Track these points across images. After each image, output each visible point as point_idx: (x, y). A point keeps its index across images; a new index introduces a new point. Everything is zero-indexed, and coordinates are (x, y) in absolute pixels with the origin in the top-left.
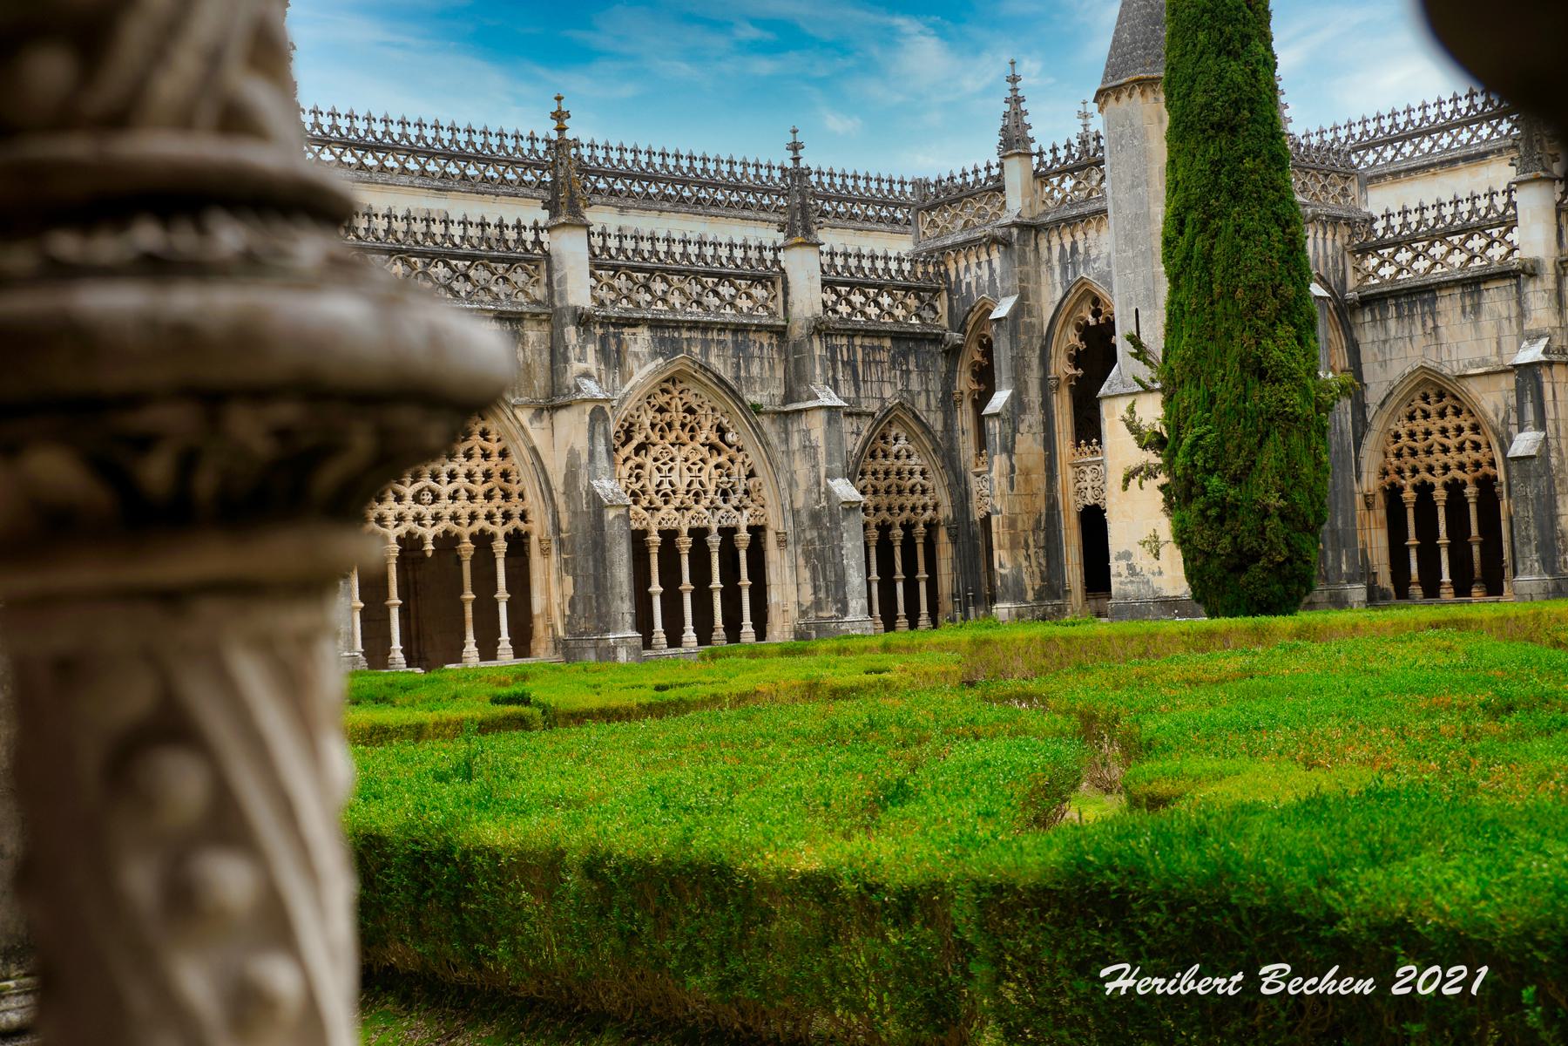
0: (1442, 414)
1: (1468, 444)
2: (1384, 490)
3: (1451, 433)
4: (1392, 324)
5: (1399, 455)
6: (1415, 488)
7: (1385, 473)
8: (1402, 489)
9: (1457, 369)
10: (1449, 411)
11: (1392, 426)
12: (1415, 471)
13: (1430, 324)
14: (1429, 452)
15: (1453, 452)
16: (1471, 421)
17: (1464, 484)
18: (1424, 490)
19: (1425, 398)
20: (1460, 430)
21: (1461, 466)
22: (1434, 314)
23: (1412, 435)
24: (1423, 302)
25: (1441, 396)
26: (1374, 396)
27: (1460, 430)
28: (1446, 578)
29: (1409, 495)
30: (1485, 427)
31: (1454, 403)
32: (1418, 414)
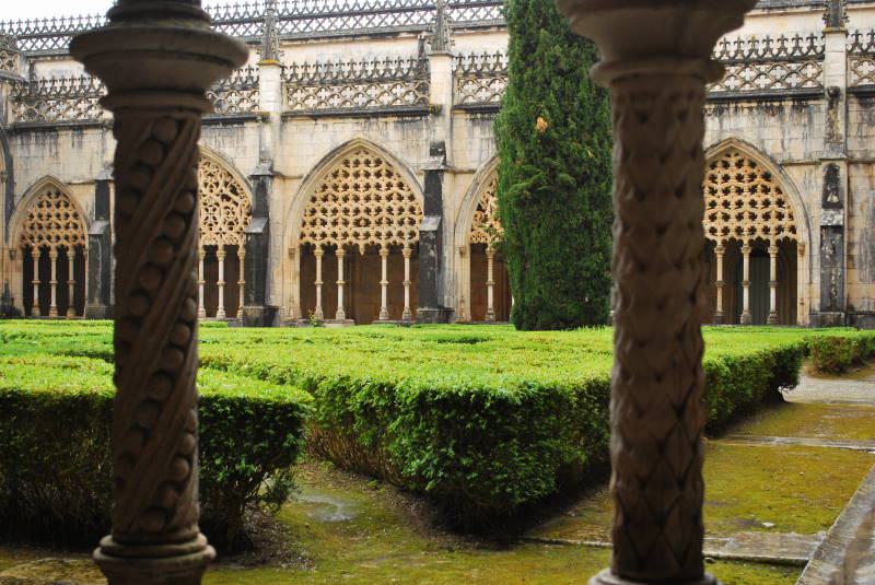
0: (58, 206)
1: (71, 225)
2: (22, 249)
3: (62, 217)
4: (32, 147)
5: (32, 228)
6: (40, 248)
7: (23, 238)
8: (32, 249)
9: (67, 180)
10: (62, 204)
11: (29, 210)
12: (40, 238)
13: (54, 150)
14: (49, 227)
15: (62, 229)
16: (73, 211)
17: (67, 249)
18: (45, 250)
19: (49, 195)
20: (67, 216)
21: (67, 238)
22: (56, 144)
23: (40, 216)
24: (52, 137)
25: (58, 194)
26: (19, 190)
27: (67, 216)
28: (53, 304)
29: (36, 253)
30: (81, 216)
31: (64, 199)
32: (45, 204)
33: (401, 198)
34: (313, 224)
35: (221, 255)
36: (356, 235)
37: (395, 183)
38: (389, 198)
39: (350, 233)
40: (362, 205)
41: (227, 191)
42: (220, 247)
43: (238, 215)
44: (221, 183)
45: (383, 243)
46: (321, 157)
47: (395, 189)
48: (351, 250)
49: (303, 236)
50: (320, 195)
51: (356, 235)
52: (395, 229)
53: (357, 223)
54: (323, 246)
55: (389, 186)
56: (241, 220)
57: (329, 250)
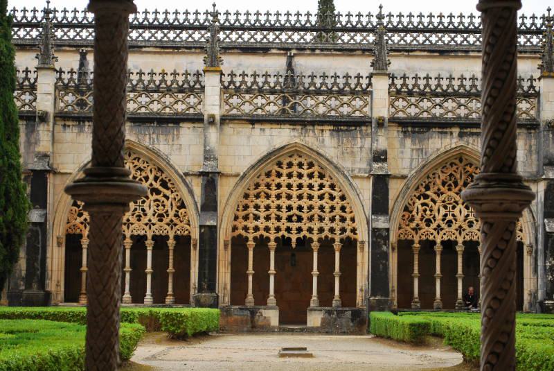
33: (332, 198)
34: (246, 218)
35: (149, 243)
36: (289, 230)
38: (321, 197)
39: (283, 227)
40: (295, 203)
41: (157, 185)
42: (149, 237)
43: (168, 206)
44: (151, 177)
45: (315, 237)
46: (259, 158)
47: (327, 189)
48: (284, 243)
49: (235, 229)
50: (253, 192)
51: (289, 230)
52: (327, 225)
53: (289, 219)
54: (255, 239)
56: (172, 213)
57: (262, 242)
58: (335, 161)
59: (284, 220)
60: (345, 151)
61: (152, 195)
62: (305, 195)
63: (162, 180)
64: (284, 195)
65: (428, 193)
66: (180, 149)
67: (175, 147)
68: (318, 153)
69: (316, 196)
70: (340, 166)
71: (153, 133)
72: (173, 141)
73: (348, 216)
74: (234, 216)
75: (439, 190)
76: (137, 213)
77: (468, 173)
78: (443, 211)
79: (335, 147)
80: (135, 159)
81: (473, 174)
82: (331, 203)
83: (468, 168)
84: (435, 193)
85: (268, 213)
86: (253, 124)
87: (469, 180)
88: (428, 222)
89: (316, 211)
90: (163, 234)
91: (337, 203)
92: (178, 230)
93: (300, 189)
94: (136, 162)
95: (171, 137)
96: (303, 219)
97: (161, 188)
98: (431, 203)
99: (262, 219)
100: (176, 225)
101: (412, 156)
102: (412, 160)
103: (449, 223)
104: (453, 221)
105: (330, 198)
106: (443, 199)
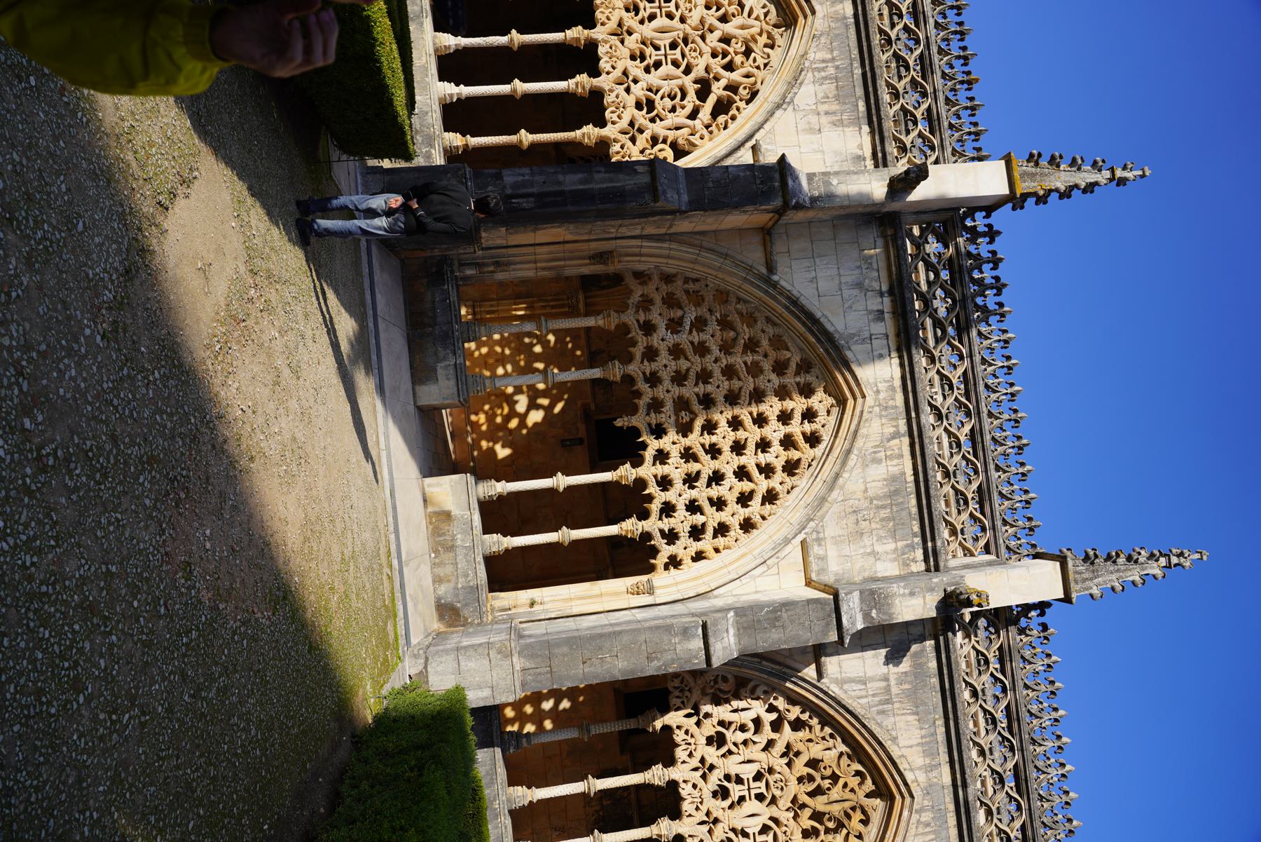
33: (744, 499)
37: (774, 482)
38: (742, 473)
41: (718, 90)
42: (596, 82)
43: (671, 119)
44: (736, 76)
46: (818, 315)
47: (762, 485)
54: (624, 329)
55: (767, 470)
58: (835, 494)
59: (676, 391)
60: (860, 515)
61: (696, 82)
62: (741, 434)
63: (731, 102)
64: (736, 384)
65: (787, 727)
66: (811, 130)
67: (813, 119)
68: (849, 452)
69: (743, 460)
70: (824, 509)
71: (837, 68)
72: (827, 113)
73: (706, 544)
74: (672, 271)
75: (797, 754)
76: (649, 50)
77: (846, 822)
78: (748, 772)
79: (866, 490)
80: (770, 36)
81: (845, 831)
82: (731, 498)
83: (858, 816)
84: (788, 746)
85: (689, 351)
86: (891, 292)
87: (831, 825)
88: (717, 740)
89: (707, 466)
90: (608, 114)
91: (733, 515)
92: (622, 147)
93: (755, 422)
94: (763, 40)
95: (835, 107)
96: (685, 436)
97: (712, 100)
98: (762, 739)
99: (672, 339)
100: (633, 140)
101: (872, 679)
102: (863, 682)
103: (722, 793)
104: (728, 802)
105: (742, 494)
106: (778, 768)
